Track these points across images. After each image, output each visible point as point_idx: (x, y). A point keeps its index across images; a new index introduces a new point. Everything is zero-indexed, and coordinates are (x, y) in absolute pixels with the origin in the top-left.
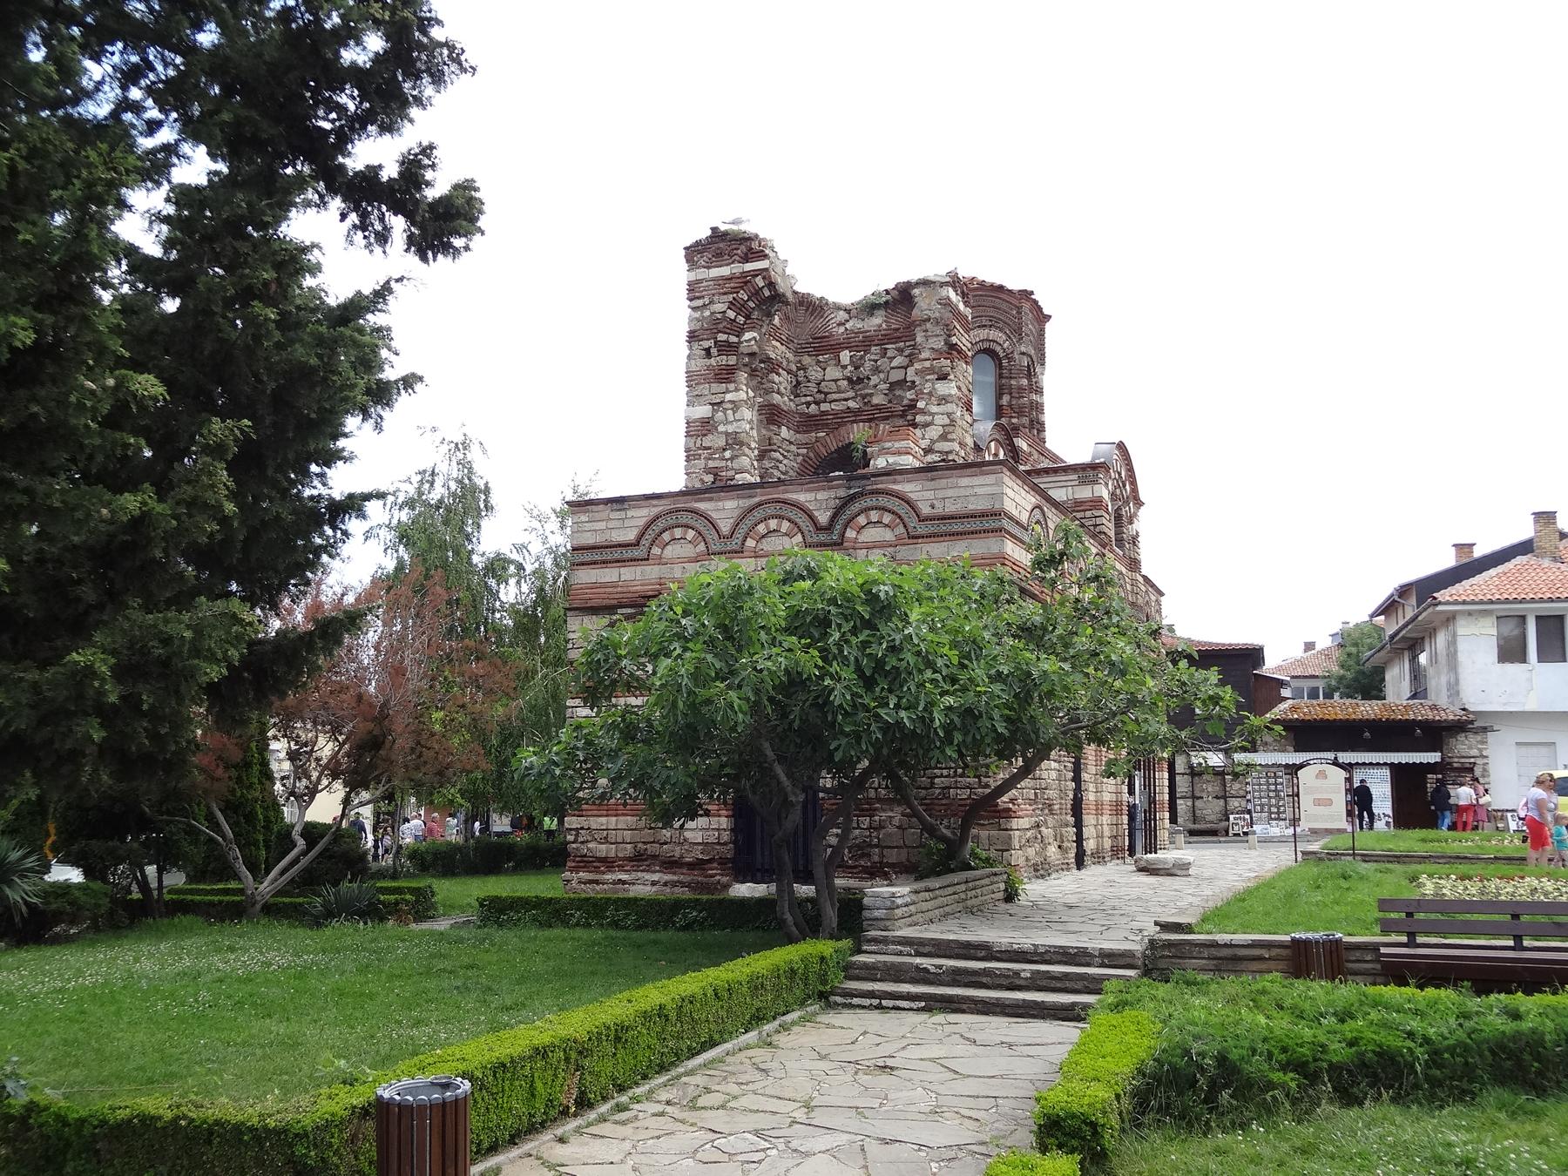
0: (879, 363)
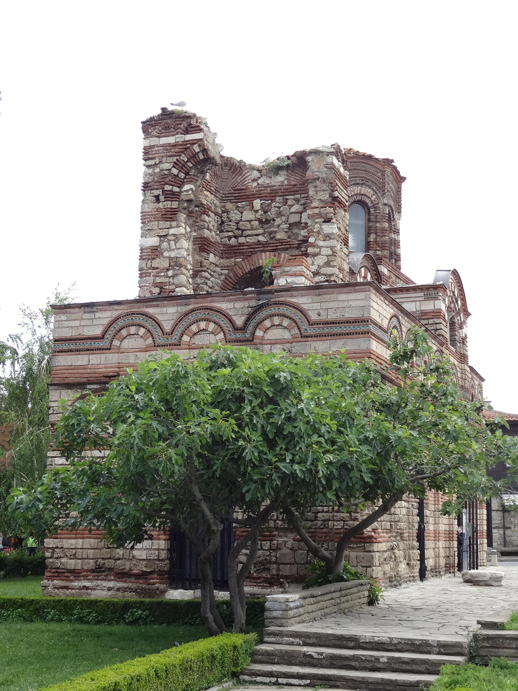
0: (281, 209)
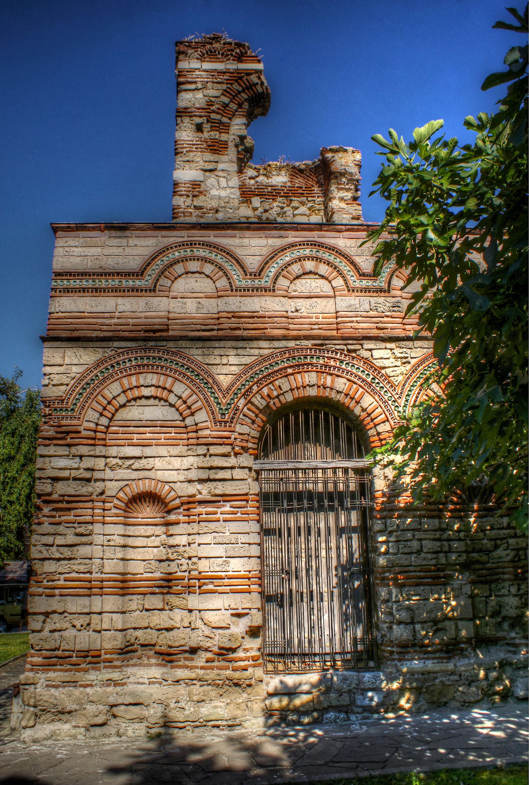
0: (285, 209)
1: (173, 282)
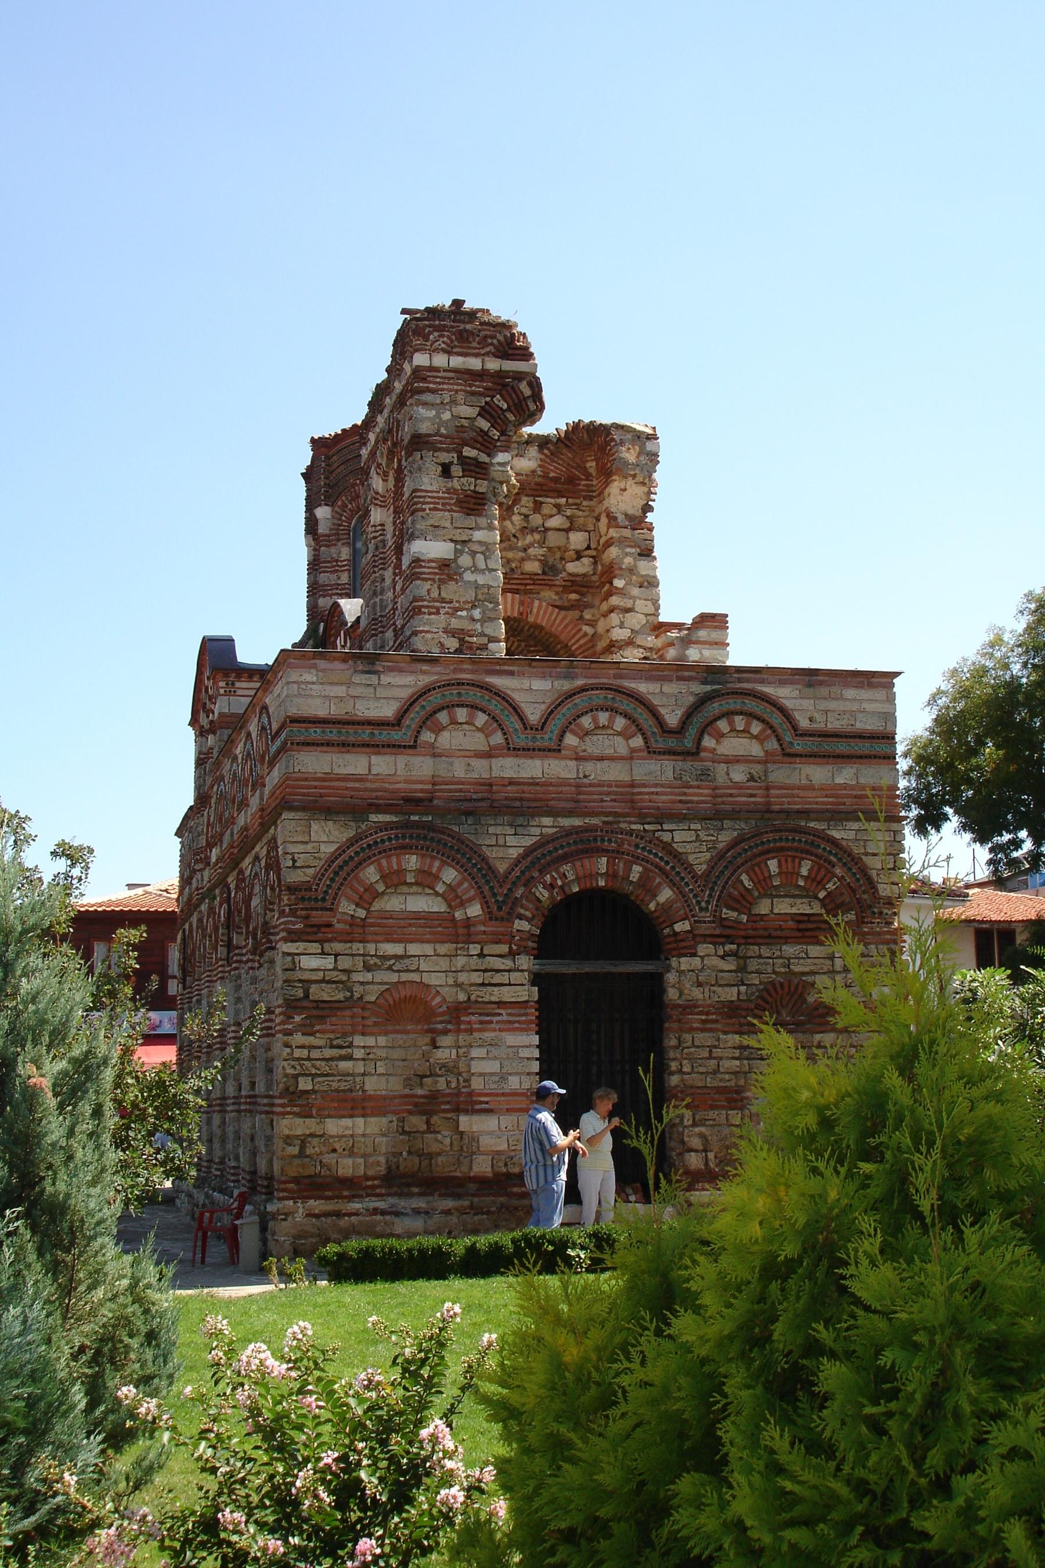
1: (437, 735)
